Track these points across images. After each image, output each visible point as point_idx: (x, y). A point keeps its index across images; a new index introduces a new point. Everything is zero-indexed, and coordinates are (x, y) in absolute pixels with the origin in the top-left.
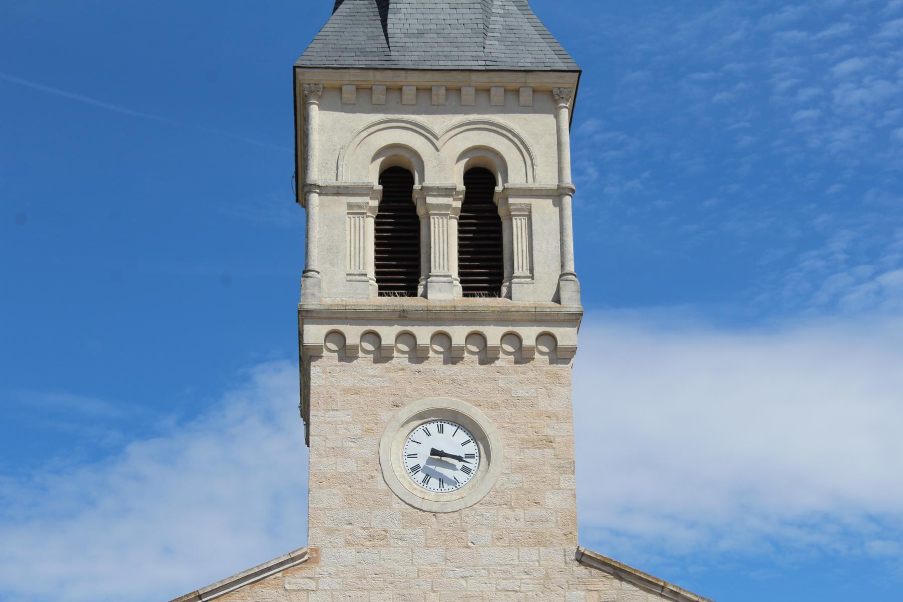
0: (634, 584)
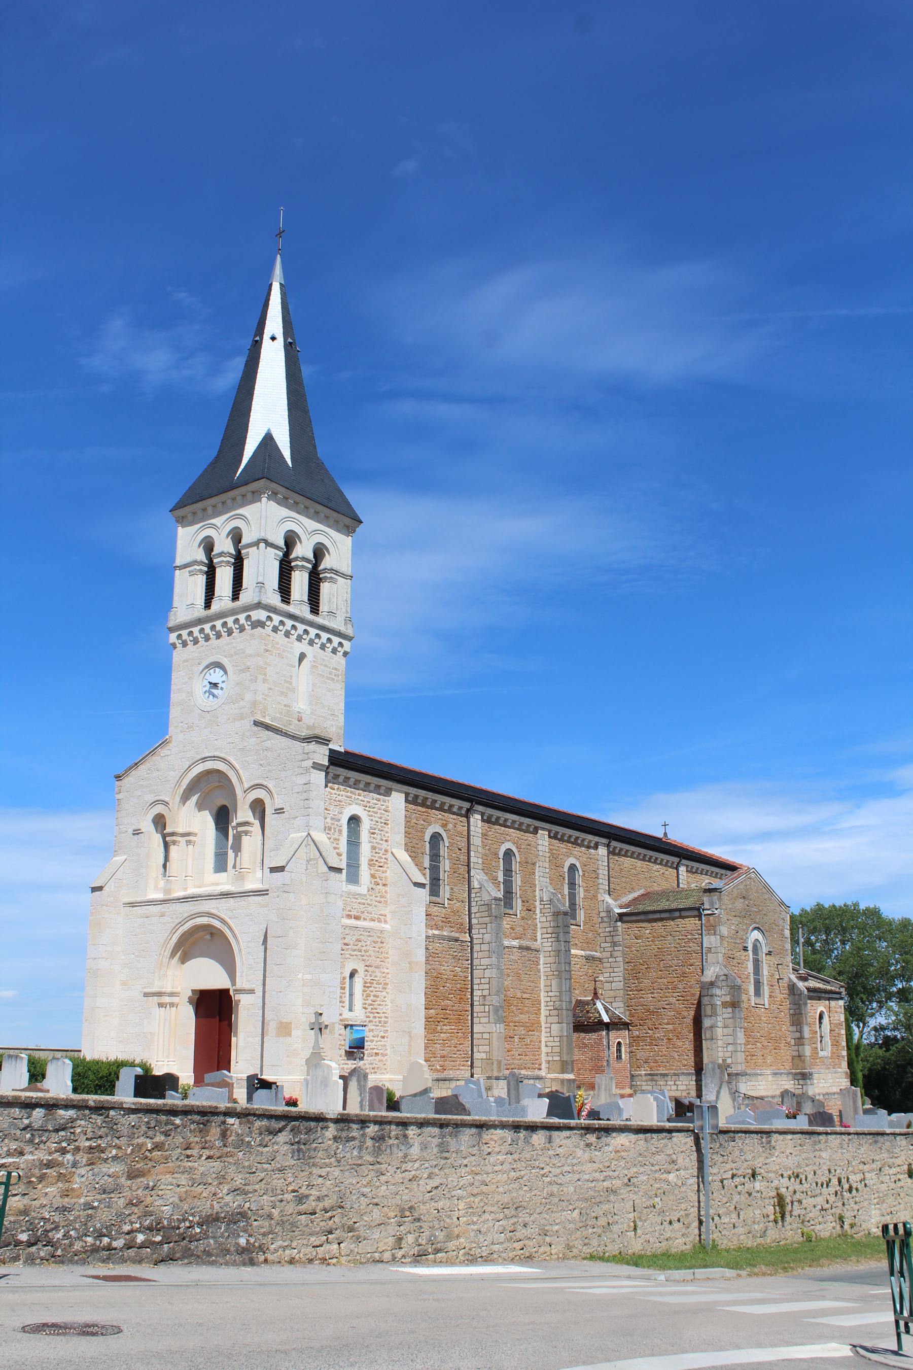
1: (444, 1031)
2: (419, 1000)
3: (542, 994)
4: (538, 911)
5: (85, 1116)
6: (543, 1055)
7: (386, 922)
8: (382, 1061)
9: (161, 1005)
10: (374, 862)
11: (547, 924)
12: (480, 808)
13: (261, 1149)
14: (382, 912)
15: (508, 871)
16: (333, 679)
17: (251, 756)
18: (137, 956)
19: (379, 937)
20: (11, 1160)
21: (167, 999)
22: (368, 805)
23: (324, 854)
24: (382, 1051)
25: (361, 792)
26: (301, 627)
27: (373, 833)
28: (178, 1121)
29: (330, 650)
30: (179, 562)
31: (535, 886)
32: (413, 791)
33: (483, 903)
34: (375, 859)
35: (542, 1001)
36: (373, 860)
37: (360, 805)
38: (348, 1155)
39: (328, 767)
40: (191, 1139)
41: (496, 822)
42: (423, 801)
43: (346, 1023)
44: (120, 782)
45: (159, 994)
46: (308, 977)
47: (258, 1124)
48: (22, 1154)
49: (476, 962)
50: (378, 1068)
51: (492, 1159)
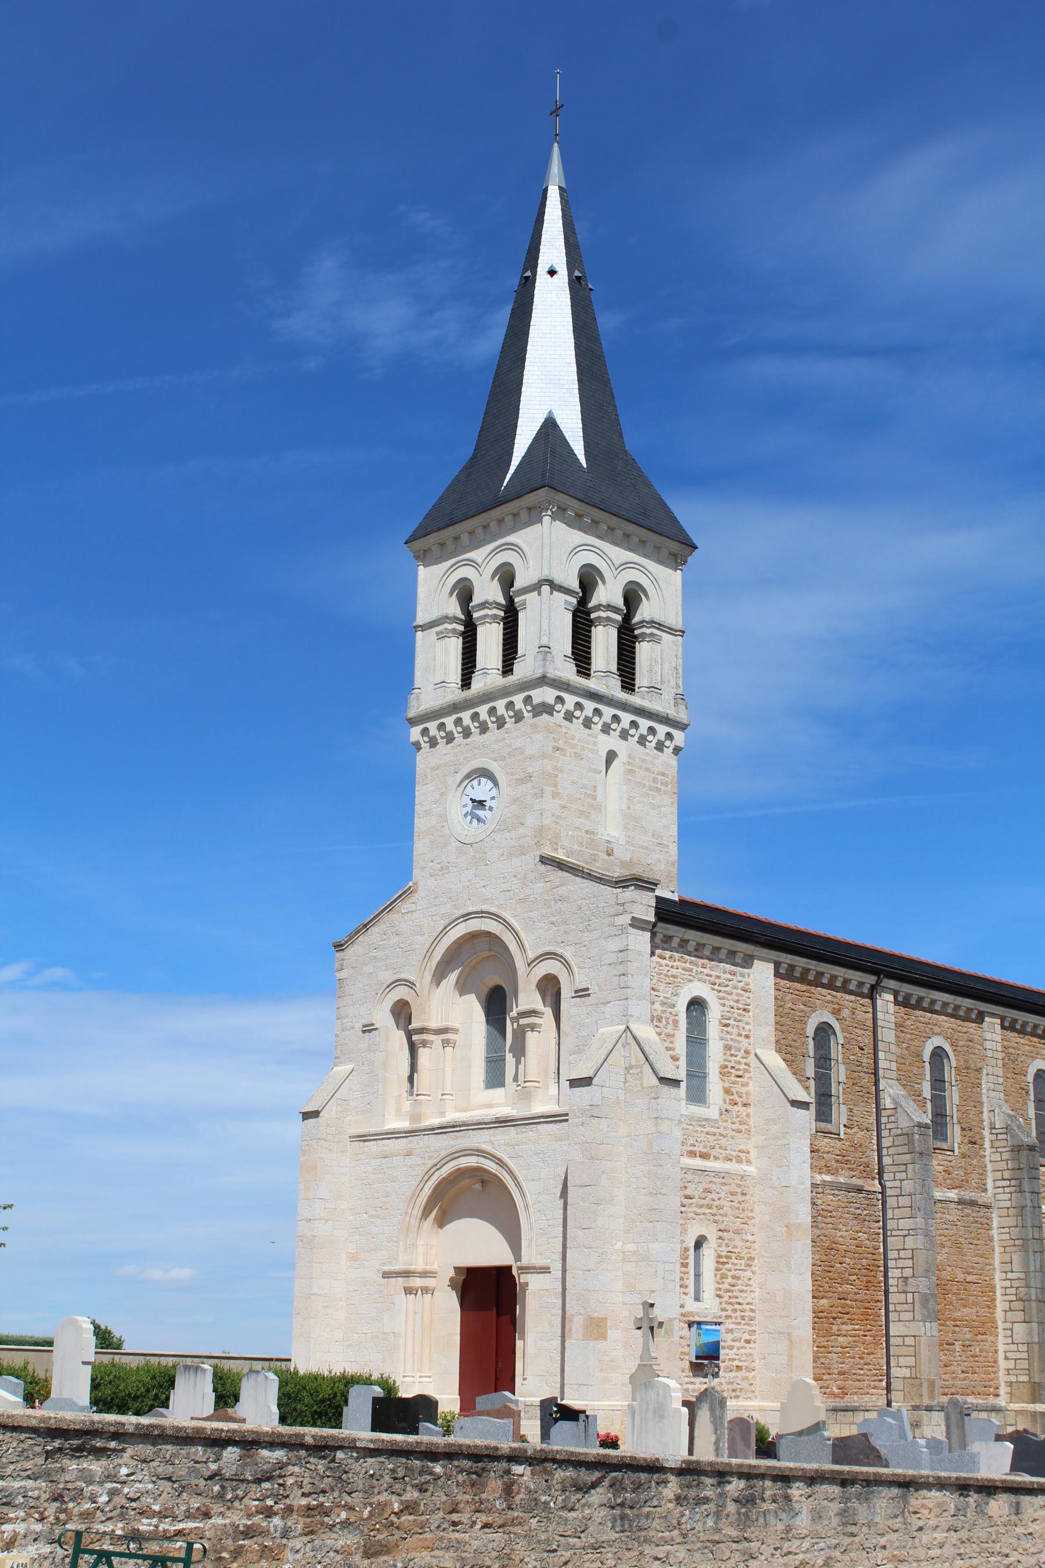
0: (569, 872)
1: (844, 1333)
2: (803, 1283)
3: (998, 1275)
4: (987, 1145)
5: (299, 1458)
6: (1002, 1374)
7: (748, 1162)
8: (747, 1378)
9: (408, 1291)
10: (729, 1069)
11: (1002, 1165)
12: (892, 984)
13: (564, 1514)
14: (743, 1147)
15: (938, 1082)
16: (658, 790)
17: (537, 909)
18: (372, 1216)
19: (738, 1186)
20: (191, 1525)
21: (417, 1282)
22: (718, 981)
23: (651, 1058)
24: (746, 1364)
25: (705, 961)
26: (608, 712)
27: (726, 1025)
28: (438, 1469)
29: (653, 744)
30: (421, 619)
31: (982, 1104)
32: (787, 959)
33: (899, 1132)
34: (730, 1064)
35: (998, 1287)
36: (726, 1067)
37: (704, 981)
38: (699, 1526)
39: (654, 925)
40: (459, 1497)
41: (918, 1006)
42: (802, 973)
43: (691, 1319)
44: (341, 953)
45: (406, 1274)
46: (631, 1247)
47: (560, 1474)
48: (207, 1515)
49: (890, 1224)
50: (741, 1389)
51: (925, 1538)
